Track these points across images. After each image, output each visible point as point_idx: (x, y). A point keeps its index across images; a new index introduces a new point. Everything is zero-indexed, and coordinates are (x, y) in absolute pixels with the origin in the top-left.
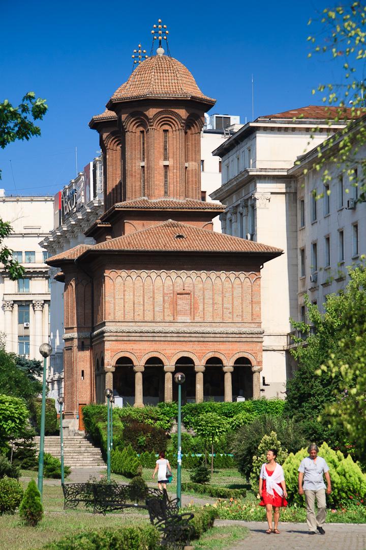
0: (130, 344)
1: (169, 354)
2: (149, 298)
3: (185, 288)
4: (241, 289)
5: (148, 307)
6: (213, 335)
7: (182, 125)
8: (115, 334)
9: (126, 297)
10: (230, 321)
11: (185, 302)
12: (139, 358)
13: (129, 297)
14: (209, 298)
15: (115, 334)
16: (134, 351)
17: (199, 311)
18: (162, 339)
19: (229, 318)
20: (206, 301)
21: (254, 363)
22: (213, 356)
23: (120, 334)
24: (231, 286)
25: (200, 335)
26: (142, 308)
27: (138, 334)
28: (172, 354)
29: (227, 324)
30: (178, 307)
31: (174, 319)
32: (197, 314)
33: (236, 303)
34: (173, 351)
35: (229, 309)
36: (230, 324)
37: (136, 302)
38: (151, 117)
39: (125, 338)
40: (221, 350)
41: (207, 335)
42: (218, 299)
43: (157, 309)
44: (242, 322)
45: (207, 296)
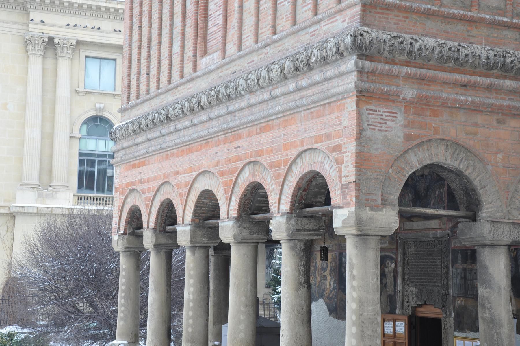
22: (251, 181)
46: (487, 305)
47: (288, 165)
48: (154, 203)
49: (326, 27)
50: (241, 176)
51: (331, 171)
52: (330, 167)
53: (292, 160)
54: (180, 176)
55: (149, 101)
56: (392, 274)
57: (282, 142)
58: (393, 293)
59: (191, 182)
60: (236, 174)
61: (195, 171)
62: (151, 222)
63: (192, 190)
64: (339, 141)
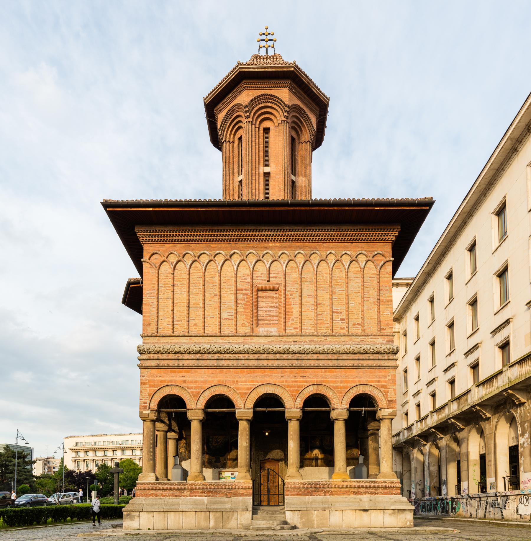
5: (212, 311)
6: (315, 356)
10: (344, 332)
11: (270, 303)
13: (181, 295)
14: (309, 296)
17: (293, 318)
19: (341, 328)
21: (382, 402)
23: (165, 356)
26: (201, 313)
28: (248, 389)
30: (260, 312)
31: (253, 331)
35: (341, 313)
36: (342, 339)
39: (171, 363)
41: (305, 357)
42: (324, 296)
43: (224, 315)
45: (305, 293)
47: (349, 389)
55: (189, 337)
59: (254, 388)
60: (303, 389)
64: (386, 384)
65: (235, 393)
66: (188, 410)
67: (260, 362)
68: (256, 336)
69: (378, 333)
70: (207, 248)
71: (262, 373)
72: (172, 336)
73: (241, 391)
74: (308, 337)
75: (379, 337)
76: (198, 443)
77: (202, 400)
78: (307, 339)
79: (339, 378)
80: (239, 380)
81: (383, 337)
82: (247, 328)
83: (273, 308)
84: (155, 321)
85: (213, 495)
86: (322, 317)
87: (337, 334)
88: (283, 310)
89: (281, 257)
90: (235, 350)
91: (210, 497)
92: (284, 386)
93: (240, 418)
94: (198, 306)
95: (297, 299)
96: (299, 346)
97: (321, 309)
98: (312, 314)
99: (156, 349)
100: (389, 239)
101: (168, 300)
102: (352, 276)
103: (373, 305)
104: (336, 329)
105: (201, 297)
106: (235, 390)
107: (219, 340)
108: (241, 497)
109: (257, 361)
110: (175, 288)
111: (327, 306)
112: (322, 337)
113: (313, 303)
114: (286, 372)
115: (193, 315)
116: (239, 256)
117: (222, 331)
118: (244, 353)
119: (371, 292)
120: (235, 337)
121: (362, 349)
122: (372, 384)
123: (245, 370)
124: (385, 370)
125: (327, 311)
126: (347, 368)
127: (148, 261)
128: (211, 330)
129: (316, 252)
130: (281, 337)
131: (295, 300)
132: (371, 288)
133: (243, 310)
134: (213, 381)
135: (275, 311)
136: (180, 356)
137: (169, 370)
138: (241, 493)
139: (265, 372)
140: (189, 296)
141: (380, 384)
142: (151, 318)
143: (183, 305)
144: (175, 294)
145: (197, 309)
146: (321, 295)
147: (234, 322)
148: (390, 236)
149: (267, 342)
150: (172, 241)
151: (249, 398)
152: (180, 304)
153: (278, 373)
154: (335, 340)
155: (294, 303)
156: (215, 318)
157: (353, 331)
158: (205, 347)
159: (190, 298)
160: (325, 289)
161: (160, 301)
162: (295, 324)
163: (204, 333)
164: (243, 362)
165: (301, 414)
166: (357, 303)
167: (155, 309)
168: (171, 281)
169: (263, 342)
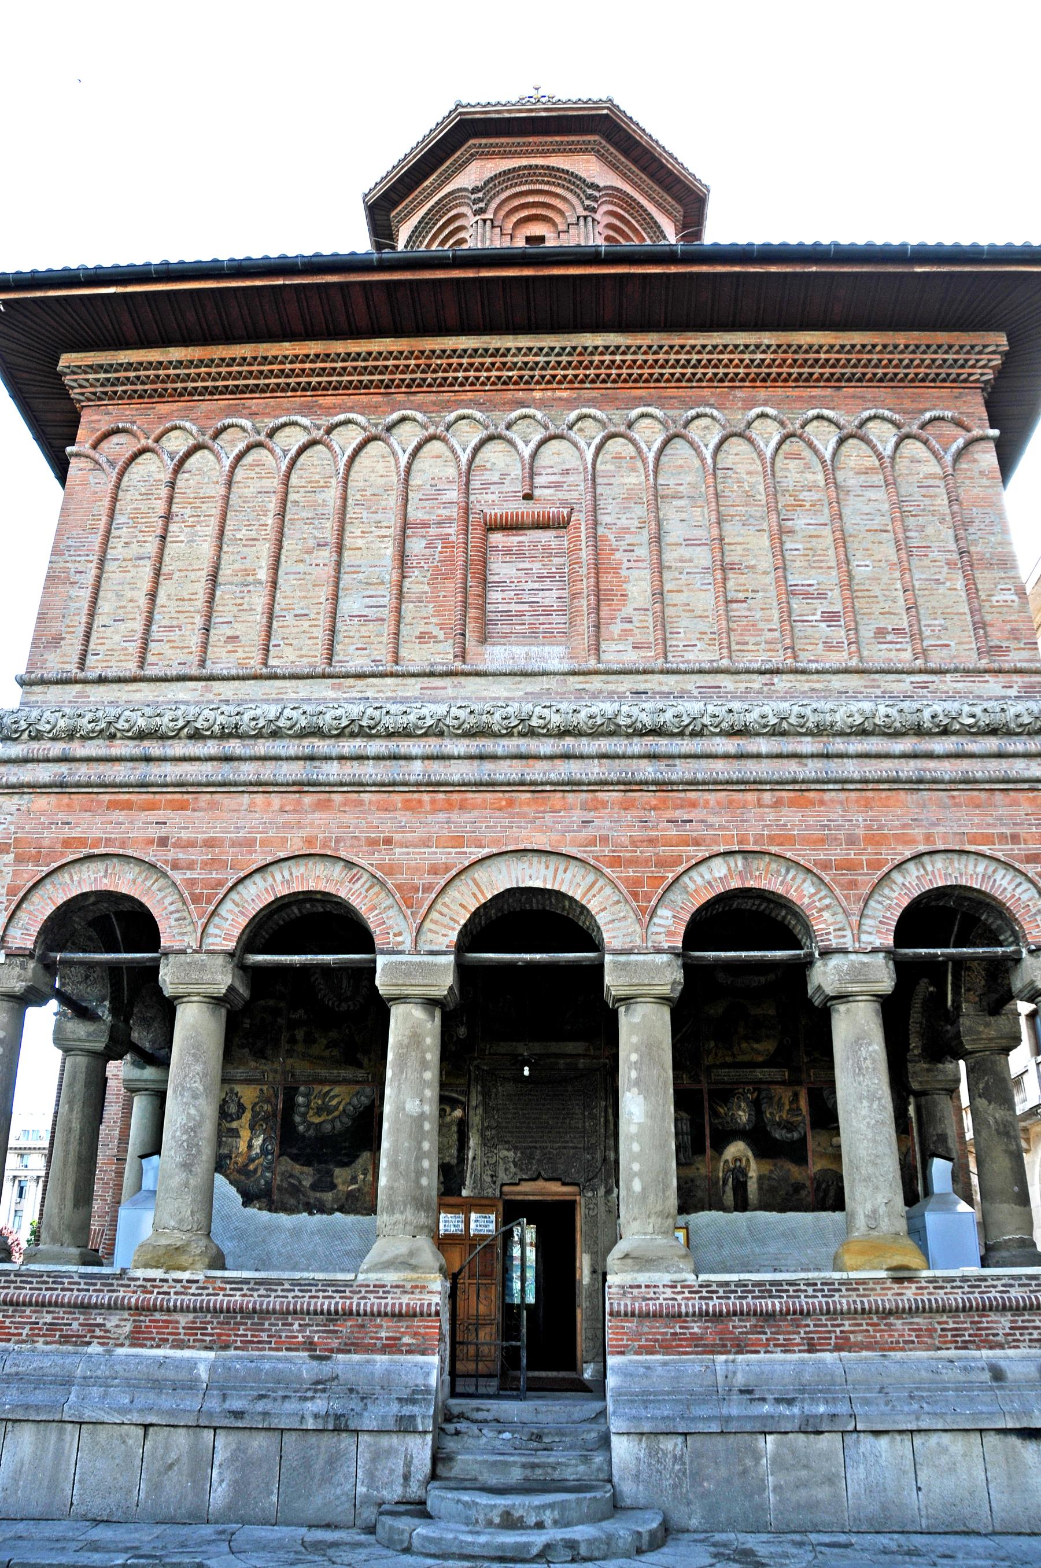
0: (152, 807)
1: (416, 870)
2: (309, 552)
3: (537, 493)
4: (880, 494)
7: (587, 202)
8: (57, 749)
9: (171, 549)
11: (536, 566)
12: (196, 899)
14: (690, 543)
15: (57, 749)
16: (172, 854)
17: (628, 610)
18: (369, 771)
19: (829, 646)
20: (670, 556)
22: (735, 884)
24: (820, 478)
25: (637, 746)
26: (259, 601)
27: (211, 748)
28: (434, 870)
29: (818, 683)
30: (494, 596)
32: (616, 628)
33: (862, 569)
34: (441, 855)
35: (822, 596)
36: (837, 682)
37: (225, 572)
38: (480, 184)
39: (120, 772)
40: (789, 840)
43: (350, 605)
44: (919, 663)
45: (675, 531)
46: (1012, 1133)
47: (885, 869)
48: (233, 895)
49: (959, 685)
50: (694, 874)
51: (1019, 890)
52: (1013, 886)
53: (896, 862)
54: (397, 850)
55: (203, 683)
56: (454, 1128)
57: (861, 832)
58: (454, 1161)
59: (460, 867)
60: (681, 869)
61: (480, 847)
62: (216, 936)
63: (457, 882)
65: (377, 889)
66: (166, 954)
67: (488, 766)
68: (477, 674)
69: (984, 663)
70: (306, 410)
71: (500, 809)
72: (135, 680)
73: (401, 878)
74: (695, 677)
75: (987, 677)
76: (195, 1097)
77: (230, 917)
78: (691, 683)
79: (838, 828)
80: (397, 837)
81: (1002, 678)
82: (440, 647)
83: (547, 584)
84: (81, 630)
85: (246, 1345)
86: (749, 610)
87: (813, 666)
88: (586, 585)
89: (575, 428)
90: (387, 721)
91: (232, 1352)
92: (596, 858)
93: (394, 991)
94: (250, 579)
95: (642, 552)
96: (660, 705)
97: (742, 581)
98: (706, 600)
99: (62, 723)
100: (972, 378)
101: (141, 562)
102: (852, 482)
103: (945, 569)
104: (810, 647)
105: (265, 549)
106: (379, 874)
107: (323, 689)
108: (385, 1358)
109: (476, 763)
110: (173, 527)
111: (765, 573)
112: (755, 676)
113: (708, 563)
114: (604, 804)
115: (227, 608)
116: (418, 428)
117: (336, 658)
118: (425, 735)
119: (930, 530)
120: (389, 681)
121: (927, 714)
122: (984, 849)
123: (426, 797)
124: (1031, 795)
125: (765, 591)
126: (871, 786)
127: (91, 453)
128: (292, 658)
129: (708, 410)
130: (581, 678)
131: (633, 556)
132: (931, 518)
133: (426, 588)
134: (284, 840)
135: (555, 594)
136: (154, 748)
137: (107, 797)
138: (383, 1335)
139: (511, 803)
140: (221, 548)
141: (1016, 849)
142: (67, 621)
143: (193, 578)
144: (169, 545)
145: (246, 589)
146: (740, 539)
147: (387, 628)
148: (973, 366)
149: (521, 693)
150: (181, 395)
151: (438, 906)
152: (183, 574)
153: (567, 808)
154: (806, 686)
155: (632, 564)
156: (312, 616)
157: (878, 655)
158: (259, 712)
159: (223, 555)
160: (751, 521)
161: (110, 566)
162: (636, 631)
163: (265, 664)
164: (417, 766)
165: (679, 975)
166: (883, 564)
167: (86, 594)
168: (161, 507)
169: (506, 694)
